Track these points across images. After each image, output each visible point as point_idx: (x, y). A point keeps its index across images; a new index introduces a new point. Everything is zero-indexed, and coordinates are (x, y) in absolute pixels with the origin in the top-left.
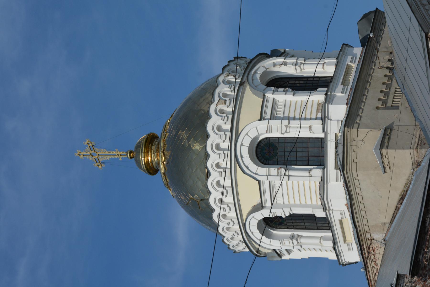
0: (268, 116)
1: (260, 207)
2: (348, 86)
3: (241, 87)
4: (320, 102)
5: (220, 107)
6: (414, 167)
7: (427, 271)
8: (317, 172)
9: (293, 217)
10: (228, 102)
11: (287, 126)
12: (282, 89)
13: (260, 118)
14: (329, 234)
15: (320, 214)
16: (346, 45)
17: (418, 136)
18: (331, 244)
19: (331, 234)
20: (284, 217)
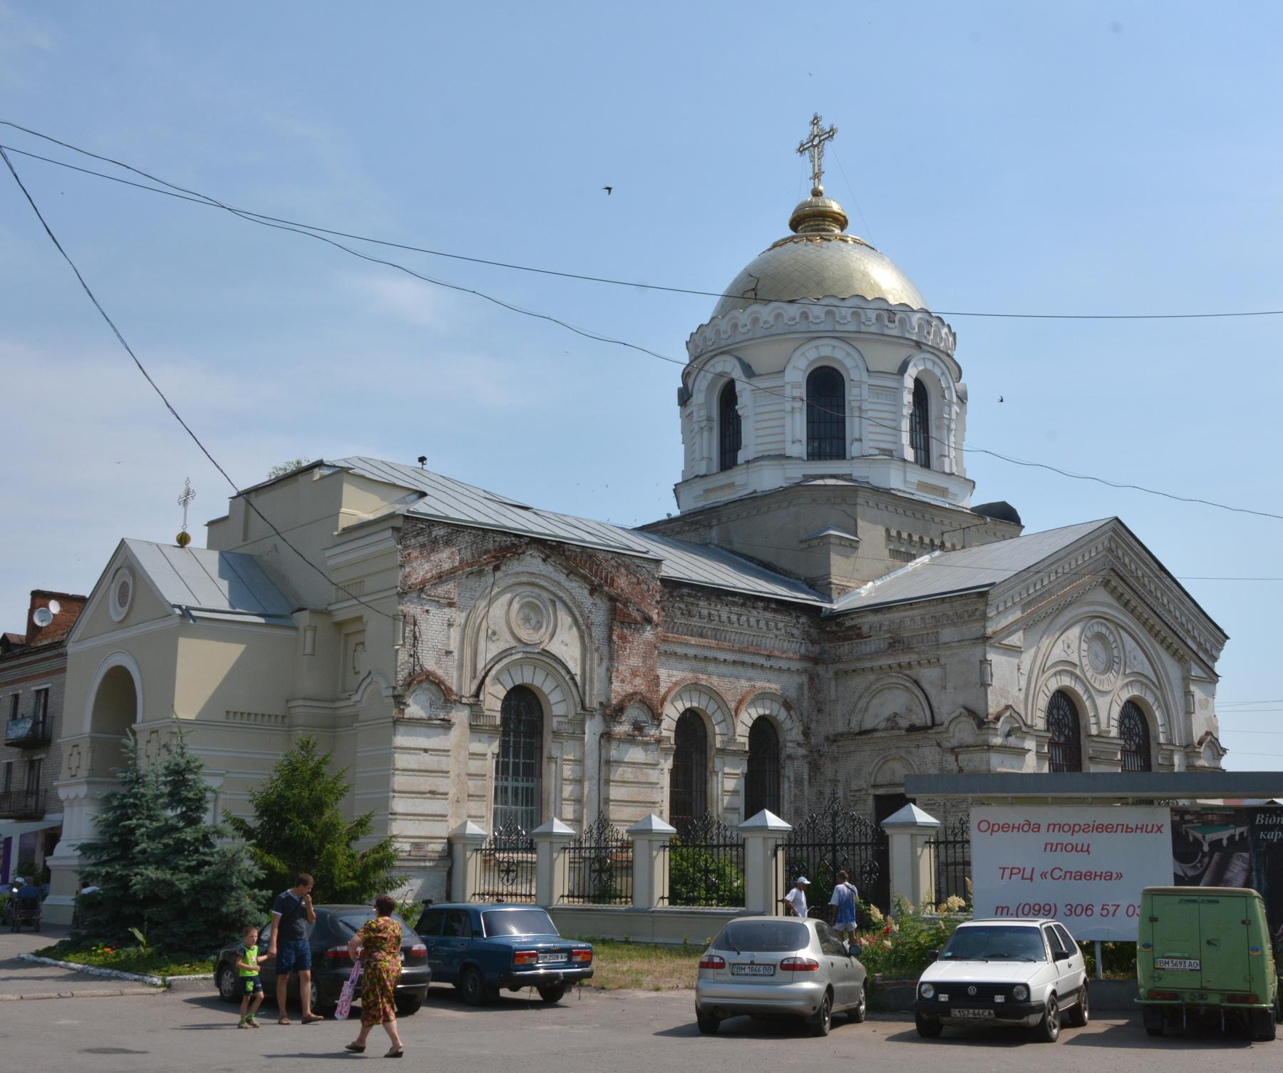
1: (749, 371)
3: (913, 343)
6: (808, 580)
7: (668, 598)
9: (737, 419)
14: (715, 466)
15: (742, 456)
16: (974, 487)
17: (848, 584)
18: (703, 472)
19: (715, 472)
20: (737, 407)
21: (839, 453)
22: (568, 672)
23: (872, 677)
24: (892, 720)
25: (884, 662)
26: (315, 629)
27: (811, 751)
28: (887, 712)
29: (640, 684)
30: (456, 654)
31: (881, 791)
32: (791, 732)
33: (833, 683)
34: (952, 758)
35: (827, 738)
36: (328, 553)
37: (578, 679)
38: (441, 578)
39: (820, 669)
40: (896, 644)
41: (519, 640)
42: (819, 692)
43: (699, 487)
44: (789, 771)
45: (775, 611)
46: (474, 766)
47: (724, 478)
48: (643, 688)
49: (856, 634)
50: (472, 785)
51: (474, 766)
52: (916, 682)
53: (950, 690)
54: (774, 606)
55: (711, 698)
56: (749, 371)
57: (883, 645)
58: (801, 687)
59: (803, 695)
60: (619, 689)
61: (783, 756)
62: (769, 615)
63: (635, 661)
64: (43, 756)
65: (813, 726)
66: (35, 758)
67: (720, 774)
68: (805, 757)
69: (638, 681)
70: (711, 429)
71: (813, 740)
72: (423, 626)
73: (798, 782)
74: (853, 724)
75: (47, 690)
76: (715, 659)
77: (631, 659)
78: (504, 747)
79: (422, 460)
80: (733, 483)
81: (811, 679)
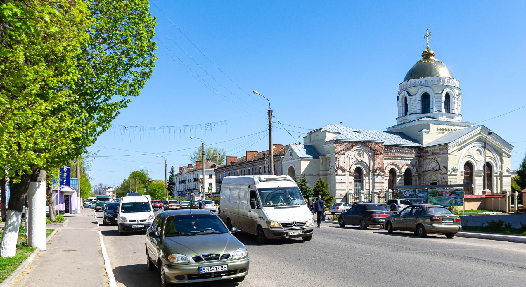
15: (408, 113)
18: (401, 116)
21: (428, 112)
22: (366, 164)
23: (430, 160)
24: (433, 169)
25: (431, 157)
26: (323, 159)
27: (418, 175)
28: (432, 167)
29: (380, 165)
30: (346, 163)
31: (431, 182)
32: (414, 171)
34: (442, 176)
35: (422, 172)
36: (324, 146)
37: (368, 165)
38: (342, 150)
39: (420, 158)
40: (434, 154)
41: (357, 159)
43: (401, 119)
44: (413, 179)
45: (410, 148)
46: (350, 181)
47: (404, 118)
48: (381, 166)
49: (426, 152)
50: (350, 184)
51: (350, 181)
52: (437, 161)
56: (409, 94)
57: (432, 154)
60: (376, 166)
61: (412, 175)
63: (379, 161)
65: (419, 170)
68: (417, 176)
69: (380, 165)
70: (403, 107)
71: (419, 172)
72: (340, 159)
73: (416, 181)
74: (427, 169)
77: (378, 161)
78: (356, 178)
79: (341, 123)
81: (418, 160)
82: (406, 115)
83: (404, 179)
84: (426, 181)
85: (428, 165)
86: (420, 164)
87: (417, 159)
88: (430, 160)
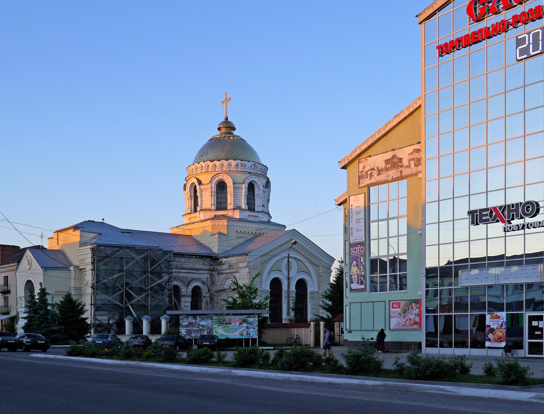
0: (235, 186)
2: (248, 218)
3: (248, 173)
4: (242, 207)
5: (240, 165)
8: (213, 207)
10: (242, 167)
11: (231, 194)
12: (247, 190)
13: (234, 182)
18: (189, 212)
23: (226, 275)
27: (210, 295)
33: (217, 276)
35: (215, 291)
39: (213, 273)
42: (213, 279)
44: (204, 300)
45: (198, 258)
47: (193, 215)
52: (234, 277)
53: (241, 279)
54: (198, 257)
55: (180, 282)
56: (200, 183)
57: (228, 267)
58: (207, 278)
59: (208, 280)
61: (202, 296)
62: (197, 259)
64: (8, 296)
66: (6, 296)
67: (183, 302)
68: (208, 296)
71: (211, 292)
73: (207, 303)
75: (7, 276)
76: (181, 272)
80: (196, 217)
81: (211, 275)
82: (195, 211)
83: (191, 300)
84: (220, 303)
85: (224, 282)
86: (213, 280)
87: (209, 273)
88: (226, 275)
